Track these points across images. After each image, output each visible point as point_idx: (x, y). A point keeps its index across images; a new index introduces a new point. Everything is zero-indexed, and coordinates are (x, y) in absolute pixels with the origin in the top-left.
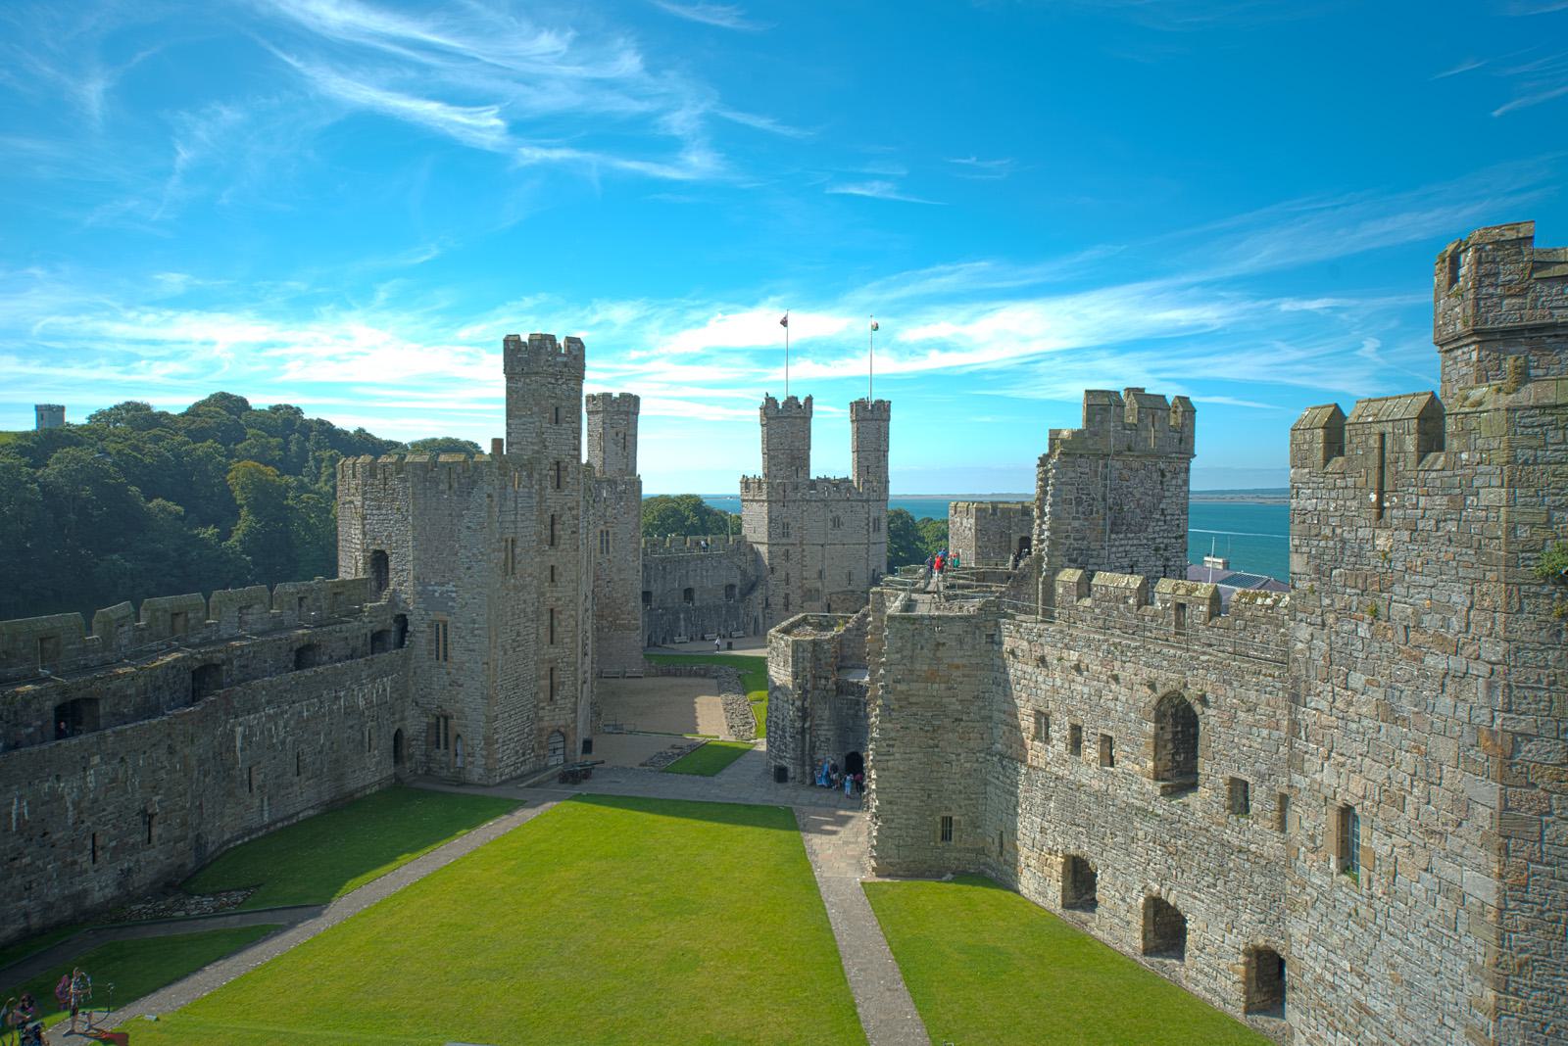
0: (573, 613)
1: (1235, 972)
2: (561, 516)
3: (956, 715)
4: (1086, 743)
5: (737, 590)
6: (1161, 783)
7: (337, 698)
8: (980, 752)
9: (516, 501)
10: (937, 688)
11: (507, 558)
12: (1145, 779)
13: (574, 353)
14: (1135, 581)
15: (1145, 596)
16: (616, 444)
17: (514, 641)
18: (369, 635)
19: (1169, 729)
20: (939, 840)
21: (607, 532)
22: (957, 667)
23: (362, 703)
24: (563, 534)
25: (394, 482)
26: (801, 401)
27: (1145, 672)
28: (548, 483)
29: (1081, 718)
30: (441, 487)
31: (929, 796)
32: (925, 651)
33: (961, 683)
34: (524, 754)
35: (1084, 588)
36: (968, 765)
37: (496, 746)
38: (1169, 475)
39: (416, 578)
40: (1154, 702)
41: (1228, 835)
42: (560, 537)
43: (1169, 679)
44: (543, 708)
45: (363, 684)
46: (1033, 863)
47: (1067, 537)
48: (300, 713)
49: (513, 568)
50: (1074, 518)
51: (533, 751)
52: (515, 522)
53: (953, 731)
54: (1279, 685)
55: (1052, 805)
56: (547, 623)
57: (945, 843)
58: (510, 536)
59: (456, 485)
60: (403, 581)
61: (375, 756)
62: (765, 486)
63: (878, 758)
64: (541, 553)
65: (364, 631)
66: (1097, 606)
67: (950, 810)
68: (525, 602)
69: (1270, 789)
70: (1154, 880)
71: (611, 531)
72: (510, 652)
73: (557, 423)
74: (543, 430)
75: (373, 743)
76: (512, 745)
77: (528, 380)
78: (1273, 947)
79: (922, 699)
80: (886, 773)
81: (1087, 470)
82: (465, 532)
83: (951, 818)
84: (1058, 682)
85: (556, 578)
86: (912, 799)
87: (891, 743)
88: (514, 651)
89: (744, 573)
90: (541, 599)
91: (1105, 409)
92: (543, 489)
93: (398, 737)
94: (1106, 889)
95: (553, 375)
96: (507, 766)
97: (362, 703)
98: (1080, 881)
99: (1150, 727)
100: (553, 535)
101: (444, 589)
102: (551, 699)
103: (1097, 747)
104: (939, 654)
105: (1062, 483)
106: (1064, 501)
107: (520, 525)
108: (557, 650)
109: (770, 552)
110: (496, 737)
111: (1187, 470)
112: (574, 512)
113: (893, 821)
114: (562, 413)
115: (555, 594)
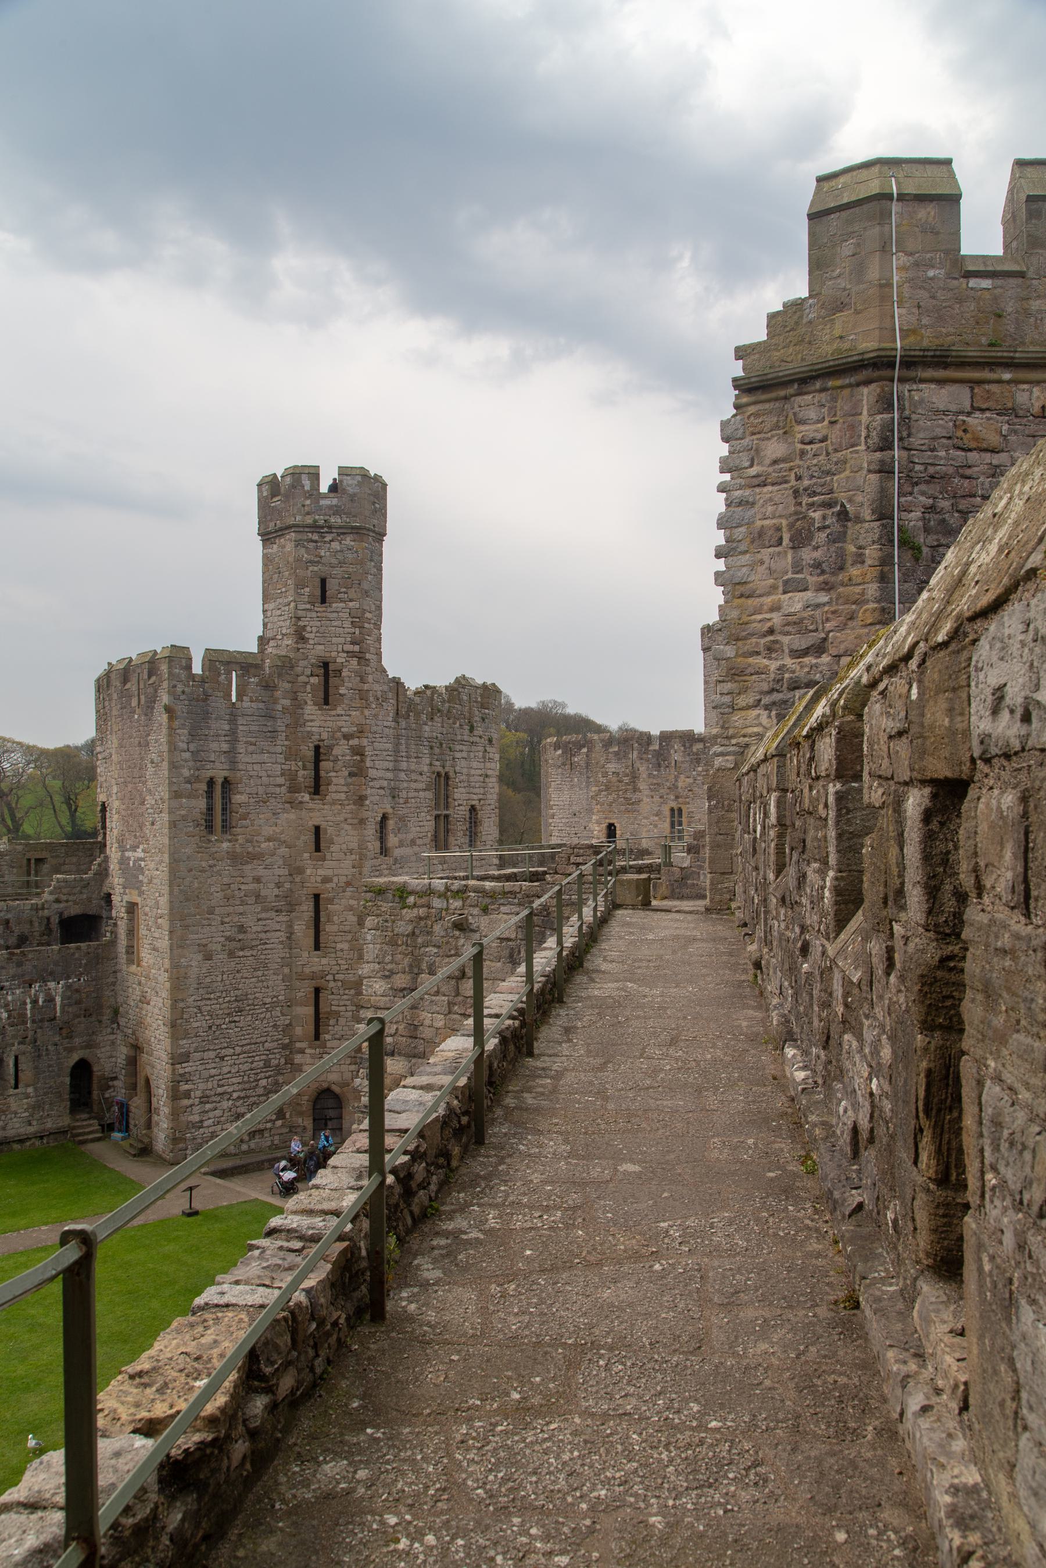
0: (353, 902)
2: (330, 748)
11: (210, 809)
13: (350, 490)
17: (229, 939)
18: (55, 920)
21: (680, 810)
37: (186, 1102)
44: (302, 1051)
50: (789, 587)
52: (231, 755)
58: (220, 775)
61: (27, 1097)
65: (46, 913)
71: (683, 807)
72: (223, 956)
73: (323, 600)
74: (300, 613)
75: (26, 1075)
76: (226, 1104)
77: (282, 540)
82: (151, 769)
85: (322, 845)
88: (231, 954)
90: (298, 879)
92: (298, 705)
93: (82, 1071)
95: (315, 527)
100: (317, 777)
101: (136, 854)
102: (317, 1037)
106: (759, 538)
107: (243, 758)
108: (324, 961)
110: (184, 1087)
112: (354, 742)
114: (332, 585)
115: (320, 872)
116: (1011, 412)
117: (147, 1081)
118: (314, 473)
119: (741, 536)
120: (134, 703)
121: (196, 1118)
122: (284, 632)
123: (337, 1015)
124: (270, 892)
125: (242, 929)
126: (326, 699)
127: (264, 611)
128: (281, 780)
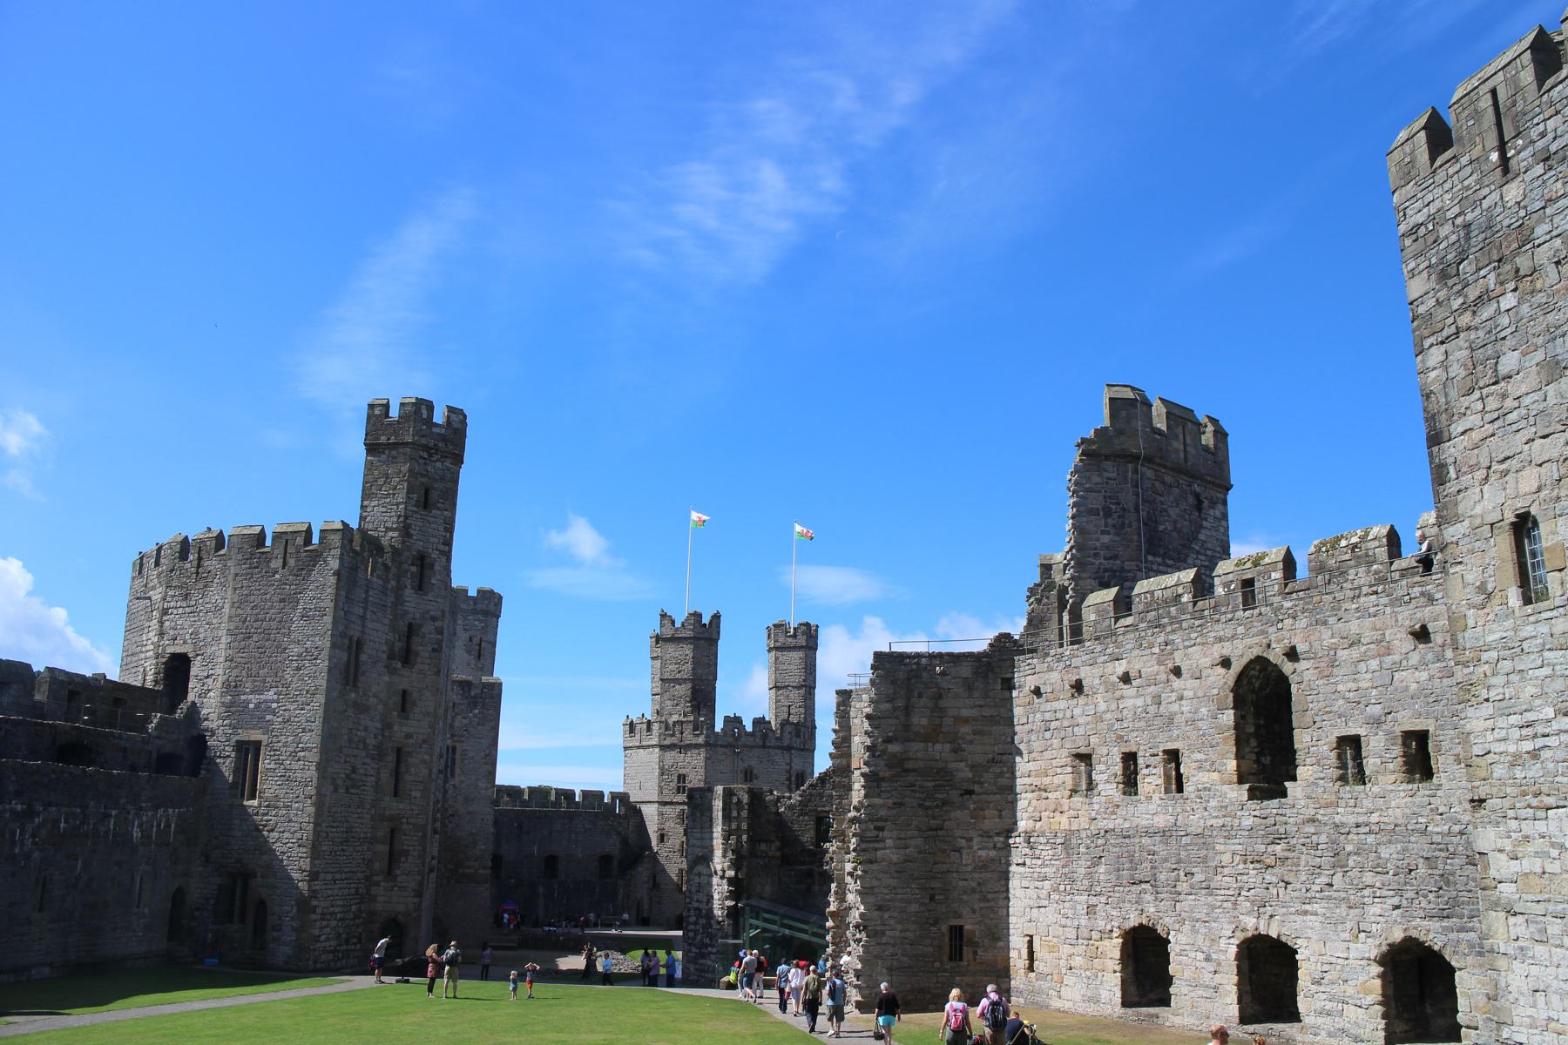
1: (1368, 992)
2: (421, 626)
3: (965, 786)
4: (1145, 771)
5: (615, 863)
6: (1247, 786)
7: (107, 816)
8: (998, 834)
9: (367, 592)
10: (940, 750)
12: (1225, 787)
14: (1188, 575)
15: (1202, 587)
16: (469, 652)
18: (155, 755)
19: (1250, 719)
20: (945, 958)
21: (454, 749)
22: (966, 721)
23: (137, 833)
24: (423, 651)
25: (211, 564)
26: (706, 620)
27: (1217, 651)
28: (408, 582)
29: (1139, 743)
30: (274, 564)
31: (932, 898)
32: (924, 701)
33: (971, 742)
34: (347, 942)
35: (1123, 605)
36: (983, 853)
37: (313, 917)
38: (1206, 504)
39: (226, 685)
40: (1231, 683)
41: (1345, 816)
42: (417, 654)
43: (1242, 651)
44: (377, 884)
45: (141, 809)
46: (1077, 961)
47: (1096, 555)
48: (57, 821)
49: (356, 680)
50: (1103, 532)
51: (360, 941)
52: (363, 618)
53: (963, 807)
54: (1384, 600)
55: (1102, 869)
56: (392, 765)
57: (953, 964)
59: (292, 562)
60: (207, 694)
62: (655, 727)
63: (864, 846)
64: (391, 671)
66: (1142, 621)
67: (960, 917)
68: (366, 729)
69: (1388, 733)
70: (1249, 913)
72: (342, 791)
76: (333, 923)
78: (1414, 934)
79: (921, 764)
80: (874, 867)
81: (1114, 475)
83: (961, 927)
84: (1102, 707)
86: (909, 902)
87: (879, 824)
89: (625, 841)
91: (1131, 403)
92: (400, 588)
93: (178, 897)
94: (1182, 963)
95: (426, 448)
96: (325, 951)
97: (137, 833)
98: (1146, 965)
99: (1228, 717)
102: (389, 873)
103: (1160, 770)
104: (942, 704)
105: (1087, 490)
106: (1092, 512)
107: (370, 625)
108: (401, 806)
109: (661, 814)
110: (314, 903)
111: (1225, 503)
112: (438, 624)
113: (883, 933)
114: (434, 495)
116: (1163, 483)
117: (262, 906)
118: (430, 406)
119: (1082, 513)
120: (276, 564)
121: (317, 932)
122: (389, 525)
123: (406, 853)
124: (371, 741)
125: (354, 770)
126: (421, 587)
127: (363, 507)
128: (385, 648)
